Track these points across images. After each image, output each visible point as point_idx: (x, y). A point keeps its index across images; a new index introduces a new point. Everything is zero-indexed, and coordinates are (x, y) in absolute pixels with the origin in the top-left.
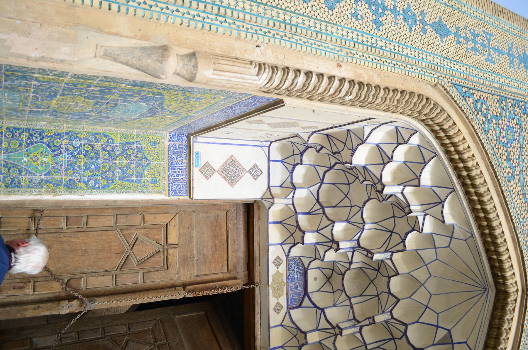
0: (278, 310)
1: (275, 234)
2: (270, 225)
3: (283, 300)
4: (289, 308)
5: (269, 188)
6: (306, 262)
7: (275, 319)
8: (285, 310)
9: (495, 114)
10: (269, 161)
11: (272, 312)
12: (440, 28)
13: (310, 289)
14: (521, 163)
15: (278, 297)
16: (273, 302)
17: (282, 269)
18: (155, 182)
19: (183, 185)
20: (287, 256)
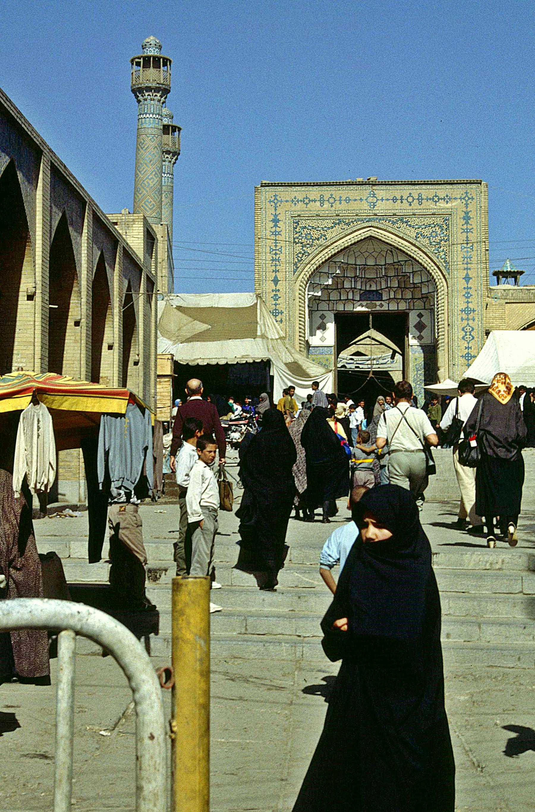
0: (381, 306)
1: (349, 308)
2: (346, 310)
3: (378, 303)
4: (382, 300)
5: (329, 310)
6: (362, 292)
7: (385, 308)
8: (382, 302)
9: (301, 247)
10: (318, 310)
11: (382, 309)
12: (276, 281)
13: (375, 289)
14: (319, 229)
15: (376, 305)
16: (378, 308)
17: (364, 303)
18: (327, 360)
19: (329, 349)
20: (359, 301)
